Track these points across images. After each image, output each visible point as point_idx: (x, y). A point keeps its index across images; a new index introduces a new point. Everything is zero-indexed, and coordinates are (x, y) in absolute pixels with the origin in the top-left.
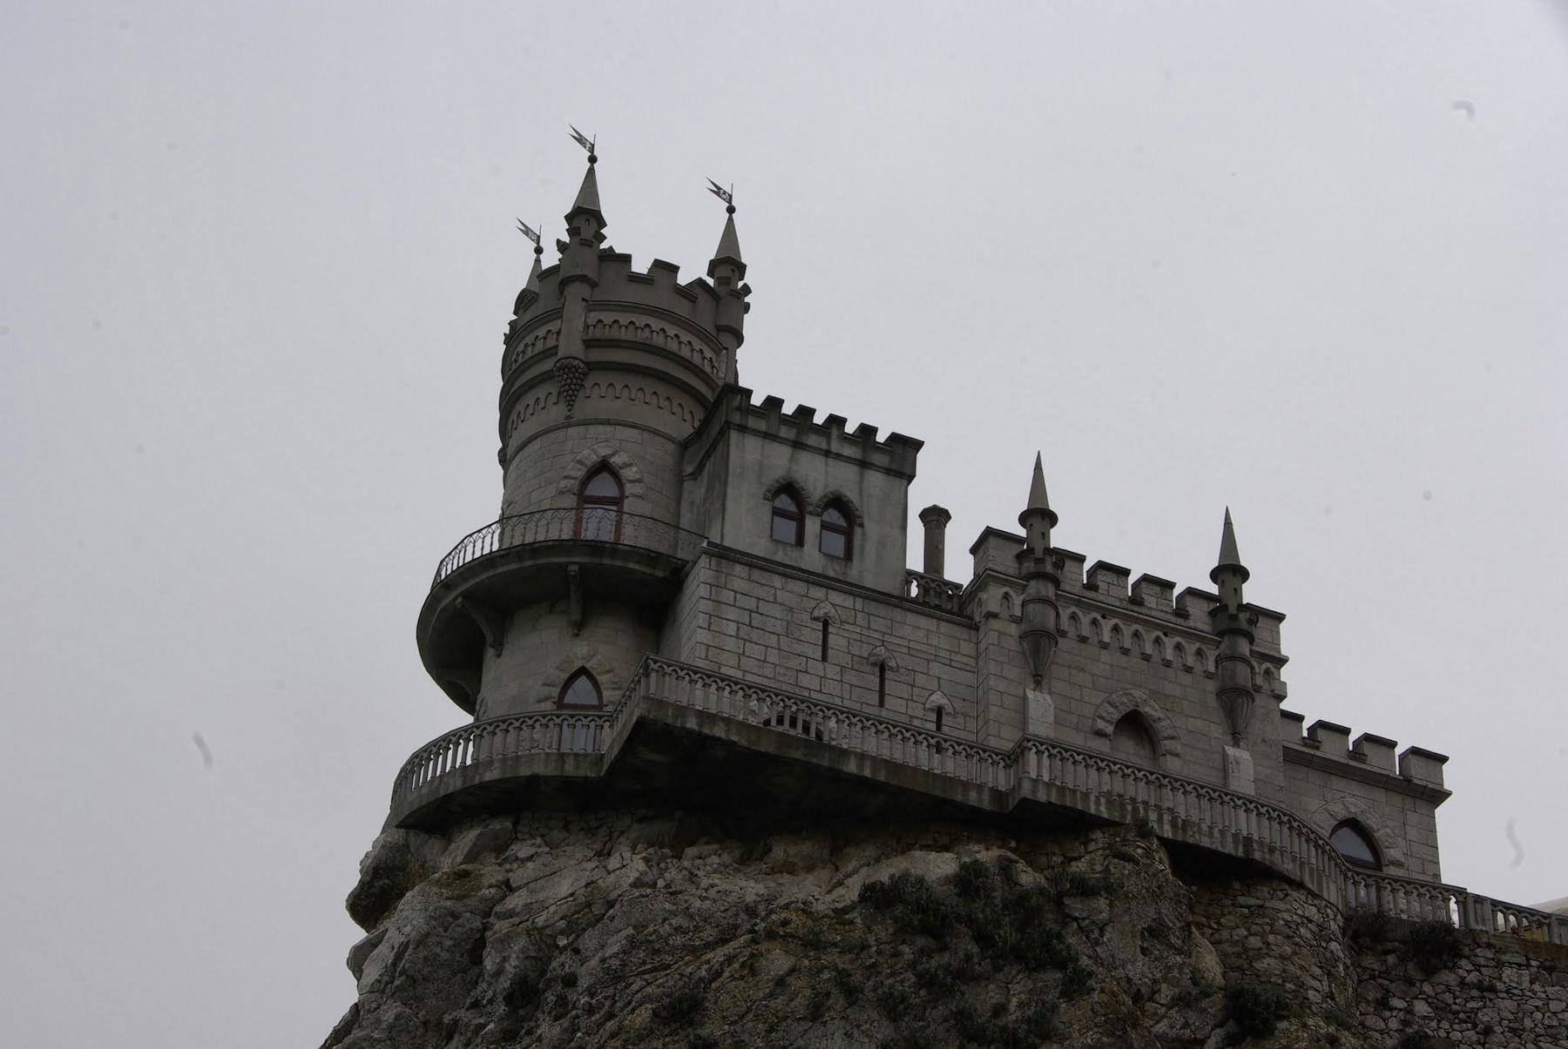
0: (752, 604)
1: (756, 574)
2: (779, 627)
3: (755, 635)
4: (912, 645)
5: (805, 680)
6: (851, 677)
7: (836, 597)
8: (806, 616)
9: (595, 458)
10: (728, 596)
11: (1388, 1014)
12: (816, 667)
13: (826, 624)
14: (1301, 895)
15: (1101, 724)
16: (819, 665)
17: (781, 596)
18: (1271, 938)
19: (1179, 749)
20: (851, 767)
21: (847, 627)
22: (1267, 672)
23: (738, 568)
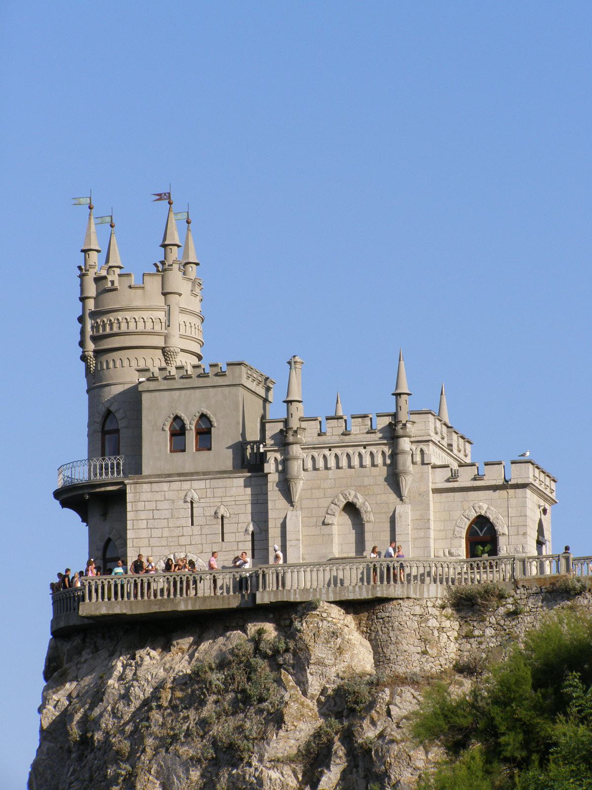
0: (152, 505)
1: (155, 486)
2: (167, 514)
3: (156, 523)
4: (237, 498)
5: (183, 541)
6: (206, 530)
7: (197, 484)
8: (181, 502)
9: (104, 410)
10: (141, 505)
11: (472, 640)
12: (188, 530)
13: (192, 503)
14: (409, 603)
15: (329, 519)
16: (189, 529)
17: (170, 495)
18: (391, 634)
19: (372, 519)
20: (182, 607)
21: (202, 500)
22: (422, 451)
23: (145, 486)
